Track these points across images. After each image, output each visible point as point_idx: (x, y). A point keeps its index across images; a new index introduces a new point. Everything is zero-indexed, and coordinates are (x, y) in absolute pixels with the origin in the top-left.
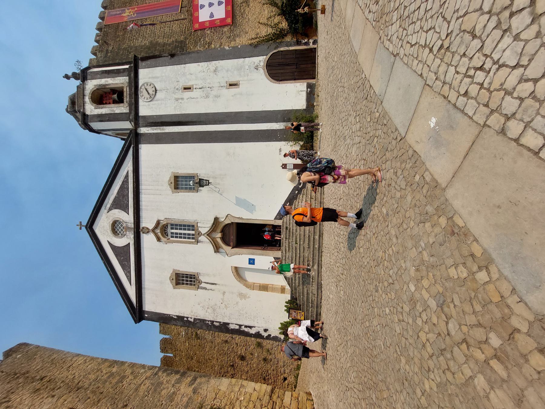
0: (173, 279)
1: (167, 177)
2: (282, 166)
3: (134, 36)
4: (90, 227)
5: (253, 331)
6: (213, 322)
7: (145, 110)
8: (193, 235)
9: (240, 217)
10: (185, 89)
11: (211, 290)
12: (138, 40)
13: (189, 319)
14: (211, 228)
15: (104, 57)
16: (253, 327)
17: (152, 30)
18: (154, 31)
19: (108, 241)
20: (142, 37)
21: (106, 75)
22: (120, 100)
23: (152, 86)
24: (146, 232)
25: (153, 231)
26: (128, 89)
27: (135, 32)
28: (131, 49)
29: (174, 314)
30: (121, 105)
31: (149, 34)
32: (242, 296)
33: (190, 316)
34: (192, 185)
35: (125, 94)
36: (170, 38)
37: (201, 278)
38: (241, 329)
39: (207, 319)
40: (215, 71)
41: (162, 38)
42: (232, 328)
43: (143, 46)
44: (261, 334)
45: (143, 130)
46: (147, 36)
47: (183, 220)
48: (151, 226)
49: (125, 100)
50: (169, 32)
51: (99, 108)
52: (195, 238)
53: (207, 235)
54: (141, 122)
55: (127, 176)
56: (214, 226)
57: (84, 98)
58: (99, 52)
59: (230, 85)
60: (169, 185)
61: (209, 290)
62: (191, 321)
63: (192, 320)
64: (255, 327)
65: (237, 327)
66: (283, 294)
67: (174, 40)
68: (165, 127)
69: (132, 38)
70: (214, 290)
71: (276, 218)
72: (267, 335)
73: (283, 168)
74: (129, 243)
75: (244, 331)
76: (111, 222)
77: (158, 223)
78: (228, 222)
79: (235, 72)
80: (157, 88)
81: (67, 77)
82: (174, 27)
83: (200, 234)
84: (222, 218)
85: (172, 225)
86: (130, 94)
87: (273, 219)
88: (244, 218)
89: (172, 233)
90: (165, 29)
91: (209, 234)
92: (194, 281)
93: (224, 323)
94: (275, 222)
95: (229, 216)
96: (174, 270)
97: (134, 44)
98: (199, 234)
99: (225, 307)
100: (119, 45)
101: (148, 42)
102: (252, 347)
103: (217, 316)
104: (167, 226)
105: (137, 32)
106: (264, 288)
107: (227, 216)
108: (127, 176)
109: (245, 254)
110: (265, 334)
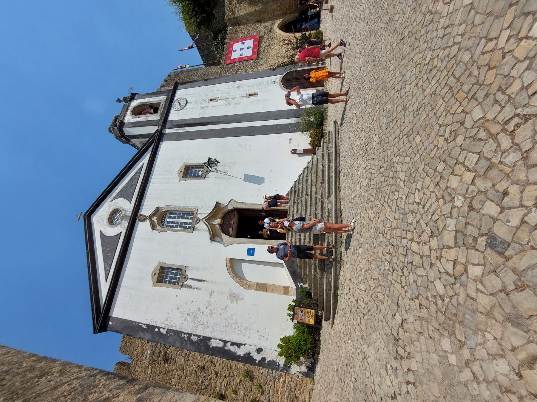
0: (155, 274)
1: (179, 166)
2: (292, 152)
5: (241, 352)
6: (190, 335)
7: (174, 116)
8: (190, 223)
9: (244, 202)
10: (211, 100)
11: (197, 288)
13: (162, 330)
16: (242, 345)
19: (100, 231)
22: (156, 111)
23: (184, 100)
24: (143, 219)
25: (151, 217)
26: (164, 103)
29: (144, 323)
30: (156, 114)
32: (234, 297)
33: (163, 326)
34: (200, 174)
37: (189, 274)
38: (226, 348)
39: (184, 331)
40: (238, 87)
42: (214, 345)
44: (251, 357)
47: (184, 207)
51: (136, 118)
52: (191, 228)
53: (205, 220)
54: (168, 125)
57: (126, 112)
59: (250, 95)
60: (178, 174)
61: (194, 288)
62: (163, 334)
63: (164, 331)
64: (245, 345)
65: (221, 345)
66: (286, 296)
68: (187, 128)
70: (200, 289)
72: (260, 359)
73: (293, 153)
75: (229, 350)
76: (111, 211)
77: (158, 209)
78: (230, 207)
79: (255, 87)
80: (188, 101)
81: (119, 101)
86: (164, 107)
89: (169, 222)
93: (204, 337)
98: (197, 221)
99: (210, 313)
102: (237, 379)
103: (197, 326)
106: (262, 287)
109: (245, 243)
110: (258, 357)
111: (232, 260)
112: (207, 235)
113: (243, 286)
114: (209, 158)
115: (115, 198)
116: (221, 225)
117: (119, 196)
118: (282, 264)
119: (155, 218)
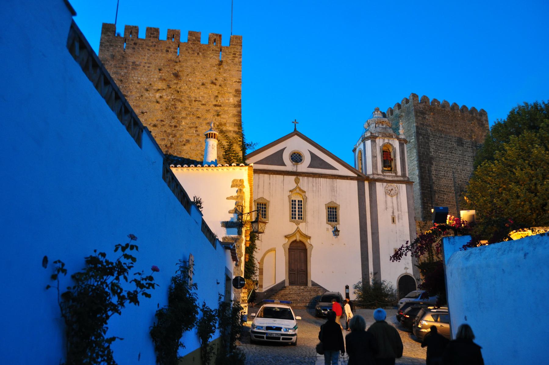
3: (437, 141)
4: (296, 133)
17: (442, 158)
18: (441, 161)
20: (436, 149)
25: (298, 187)
27: (441, 141)
28: (427, 138)
31: (439, 155)
36: (435, 177)
41: (436, 169)
43: (429, 149)
45: (366, 183)
46: (437, 153)
50: (440, 175)
67: (434, 180)
71: (312, 281)
73: (346, 286)
74: (285, 165)
82: (445, 180)
87: (312, 279)
89: (295, 201)
90: (442, 171)
91: (298, 231)
96: (269, 202)
97: (430, 141)
107: (311, 245)
109: (286, 258)
114: (339, 231)
116: (295, 241)
117: (313, 156)
118: (275, 283)
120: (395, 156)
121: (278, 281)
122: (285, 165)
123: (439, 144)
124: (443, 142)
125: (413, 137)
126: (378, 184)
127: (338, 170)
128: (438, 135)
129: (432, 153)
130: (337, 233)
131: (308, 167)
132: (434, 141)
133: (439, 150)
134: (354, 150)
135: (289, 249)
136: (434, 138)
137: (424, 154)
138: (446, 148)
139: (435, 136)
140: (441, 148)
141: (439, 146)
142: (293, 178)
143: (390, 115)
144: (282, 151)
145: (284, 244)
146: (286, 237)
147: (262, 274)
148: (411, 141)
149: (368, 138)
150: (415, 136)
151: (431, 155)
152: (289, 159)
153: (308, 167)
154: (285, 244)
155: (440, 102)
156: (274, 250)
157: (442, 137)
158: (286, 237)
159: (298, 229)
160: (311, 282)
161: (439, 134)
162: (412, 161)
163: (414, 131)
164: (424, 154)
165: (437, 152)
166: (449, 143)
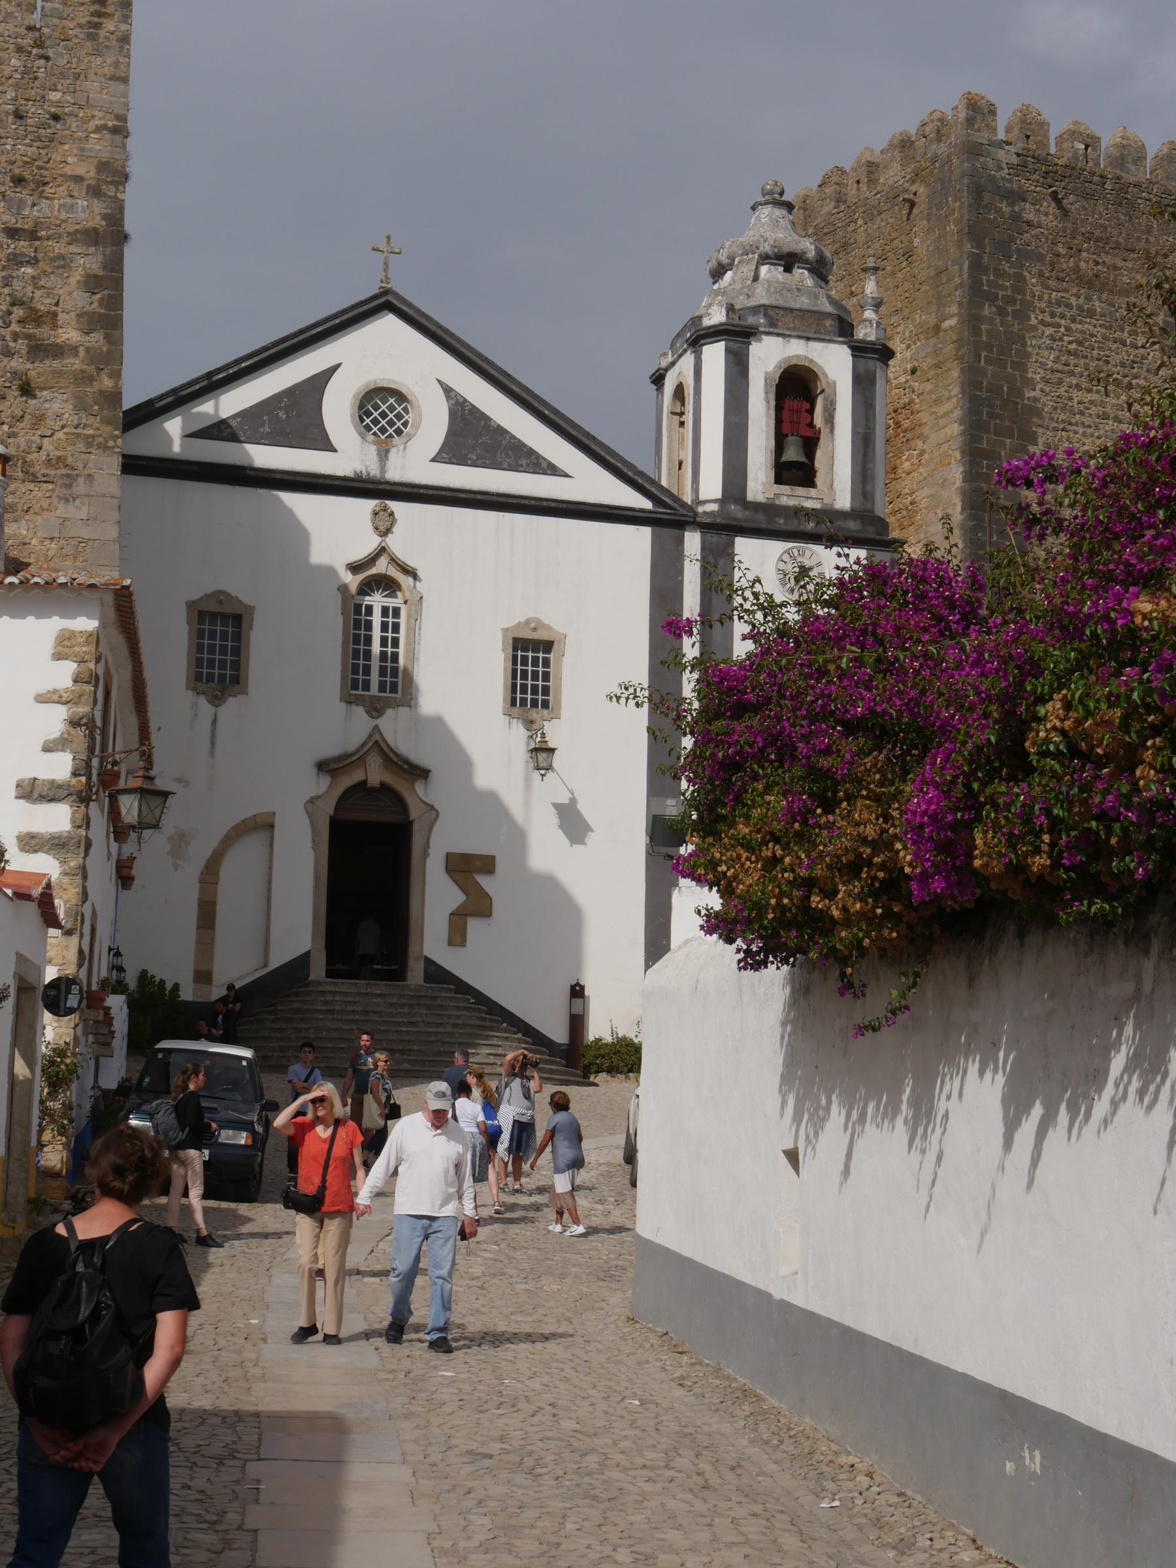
0: (221, 602)
2: (578, 984)
3: (1068, 329)
8: (367, 686)
9: (431, 851)
12: (1051, 348)
14: (396, 754)
15: (993, 179)
17: (1082, 413)
18: (1076, 424)
20: (1059, 367)
21: (862, 430)
26: (817, 505)
28: (1016, 315)
35: (801, 491)
43: (1023, 368)
45: (693, 542)
48: (396, 543)
49: (785, 489)
54: (715, 539)
55: (552, 470)
56: (406, 767)
58: (1018, 155)
60: (528, 622)
69: (1063, 317)
71: (429, 962)
73: (573, 987)
74: (331, 449)
76: (404, 390)
77: (412, 573)
78: (414, 813)
83: (375, 709)
84: (426, 789)
85: (397, 612)
87: (425, 953)
88: (428, 861)
89: (369, 610)
91: (377, 746)
92: (210, 678)
94: (417, 959)
95: (434, 813)
96: (251, 610)
97: (1035, 328)
98: (375, 709)
100: (1040, 258)
101: (1037, 393)
104: (392, 595)
105: (1080, 343)
107: (432, 808)
108: (552, 470)
109: (316, 861)
111: (271, 827)
112: (332, 748)
113: (206, 867)
114: (552, 750)
115: (448, 391)
116: (363, 783)
119: (382, 566)
120: (830, 420)
121: (280, 956)
122: (331, 449)
123: (1074, 346)
124: (1092, 335)
125: (954, 309)
126: (745, 547)
127: (567, 476)
128: (1073, 301)
129: (1038, 387)
130: (542, 756)
131: (433, 460)
132: (1049, 331)
133: (1071, 373)
134: (658, 379)
135: (331, 817)
136: (1053, 315)
137: (995, 389)
138: (1107, 362)
139: (1058, 304)
140: (1082, 361)
141: (1074, 354)
142: (370, 504)
143: (864, 187)
144: (319, 382)
145: (311, 801)
146: (323, 766)
147: (213, 927)
148: (947, 324)
149: (715, 333)
150: (960, 304)
151: (1029, 394)
152: (352, 417)
153: (433, 460)
154: (318, 797)
155: (1098, 140)
156: (264, 825)
157: (1091, 313)
158: (323, 766)
159: (377, 737)
160: (421, 964)
161: (1078, 296)
162: (942, 422)
163: (957, 280)
164: (995, 389)
165: (1060, 382)
166: (1123, 343)
